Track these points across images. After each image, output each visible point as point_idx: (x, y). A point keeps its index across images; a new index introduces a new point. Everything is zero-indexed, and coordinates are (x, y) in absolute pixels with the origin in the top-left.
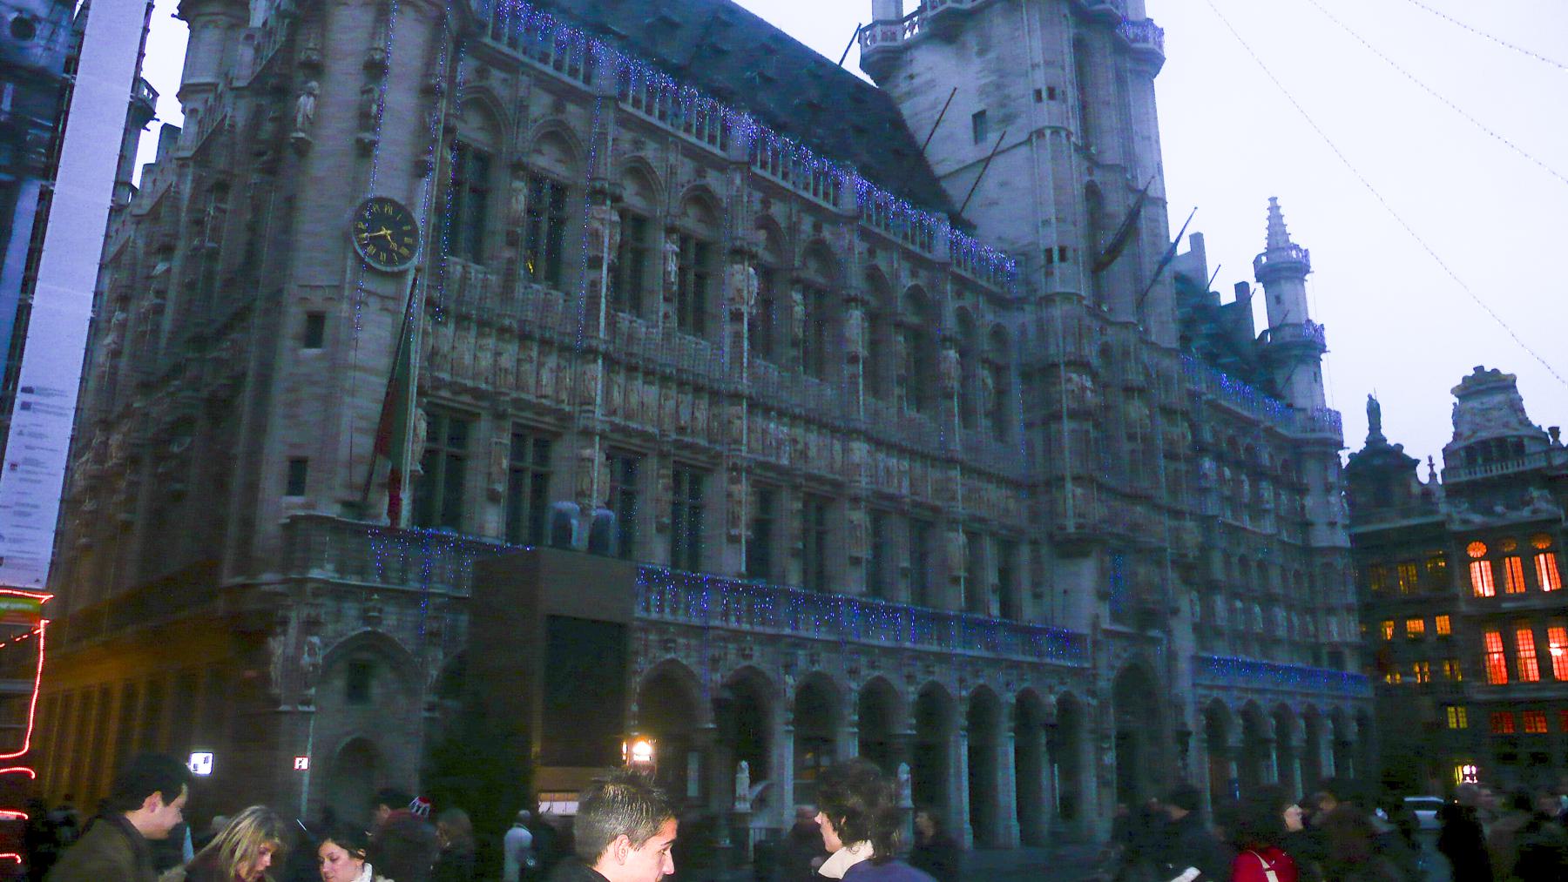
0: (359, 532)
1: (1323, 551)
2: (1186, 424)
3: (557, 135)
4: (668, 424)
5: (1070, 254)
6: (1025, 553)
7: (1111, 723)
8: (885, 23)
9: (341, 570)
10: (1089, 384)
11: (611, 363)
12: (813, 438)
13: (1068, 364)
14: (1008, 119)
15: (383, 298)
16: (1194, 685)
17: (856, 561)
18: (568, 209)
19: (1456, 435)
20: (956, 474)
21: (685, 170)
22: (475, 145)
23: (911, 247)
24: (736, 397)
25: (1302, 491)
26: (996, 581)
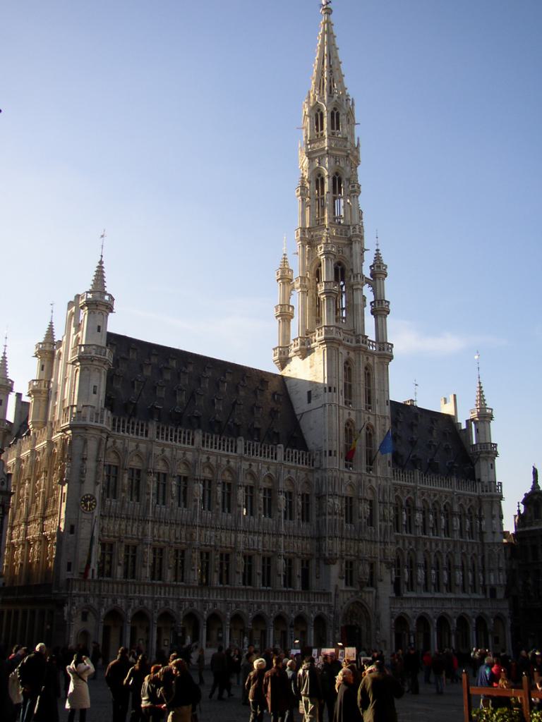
1: (489, 544)
2: (391, 508)
4: (172, 536)
6: (313, 563)
7: (341, 624)
8: (279, 347)
9: (80, 590)
10: (337, 502)
11: (154, 522)
12: (223, 535)
13: (329, 495)
14: (317, 396)
15: (88, 520)
16: (390, 608)
18: (141, 476)
20: (282, 539)
22: (113, 464)
23: (266, 460)
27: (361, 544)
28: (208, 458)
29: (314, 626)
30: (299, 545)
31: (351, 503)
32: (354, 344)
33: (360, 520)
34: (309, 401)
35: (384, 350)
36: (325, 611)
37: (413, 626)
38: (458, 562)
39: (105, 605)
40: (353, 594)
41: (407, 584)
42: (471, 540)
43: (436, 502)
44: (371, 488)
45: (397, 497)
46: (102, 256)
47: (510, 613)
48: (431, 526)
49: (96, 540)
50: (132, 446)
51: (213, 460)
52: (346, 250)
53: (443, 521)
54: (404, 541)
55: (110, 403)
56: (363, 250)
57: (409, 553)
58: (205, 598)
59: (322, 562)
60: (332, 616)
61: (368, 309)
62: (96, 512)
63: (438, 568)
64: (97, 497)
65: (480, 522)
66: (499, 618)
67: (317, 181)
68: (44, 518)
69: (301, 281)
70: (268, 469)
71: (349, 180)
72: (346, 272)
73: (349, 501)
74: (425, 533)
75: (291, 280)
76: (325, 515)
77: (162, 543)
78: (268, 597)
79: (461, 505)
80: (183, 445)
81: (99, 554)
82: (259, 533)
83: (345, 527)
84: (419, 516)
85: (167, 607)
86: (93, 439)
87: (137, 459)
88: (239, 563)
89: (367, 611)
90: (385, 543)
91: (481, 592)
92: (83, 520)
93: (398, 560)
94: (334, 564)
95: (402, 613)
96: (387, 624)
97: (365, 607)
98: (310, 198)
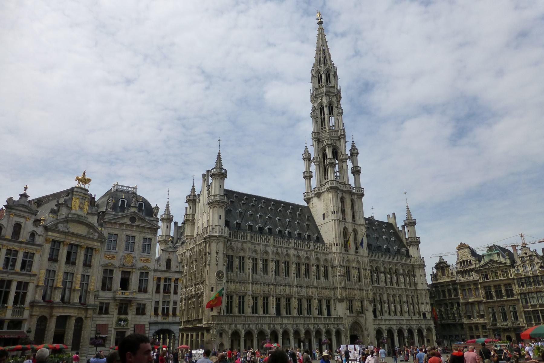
0: (220, 316)
2: (369, 272)
3: (243, 249)
5: (338, 245)
6: (332, 302)
8: (308, 192)
10: (342, 269)
11: (252, 284)
12: (287, 288)
14: (328, 216)
15: (220, 284)
17: (295, 308)
19: (458, 259)
21: (263, 248)
23: (305, 249)
24: (273, 285)
25: (414, 276)
26: (326, 308)
27: (356, 291)
28: (277, 250)
29: (335, 336)
30: (324, 293)
31: (349, 269)
32: (345, 189)
33: (354, 279)
34: (324, 218)
35: (359, 191)
36: (341, 327)
37: (385, 334)
38: (404, 299)
39: (231, 328)
40: (354, 318)
41: (380, 312)
42: (410, 288)
43: (391, 268)
44: (358, 262)
45: (371, 266)
46: (219, 150)
47: (435, 327)
48: (389, 281)
49: (224, 294)
50: (239, 245)
51: (280, 250)
52: (338, 143)
53: (395, 277)
54: (376, 289)
55: (227, 224)
56: (346, 142)
57: (379, 296)
58: (280, 323)
59: (336, 301)
60: (344, 330)
61: (350, 171)
62: (224, 279)
63: (395, 303)
64: (224, 272)
65: (414, 278)
66: (429, 330)
67: (321, 109)
68: (195, 285)
69: (316, 159)
70: (307, 254)
71: (337, 107)
72: (338, 154)
73: (348, 269)
74: (386, 284)
75: (310, 159)
76: (337, 276)
77: (257, 294)
78: (312, 321)
79: (403, 270)
80: (264, 243)
81: (226, 302)
82: (304, 287)
83: (347, 282)
84: (382, 276)
85: (262, 328)
86: (221, 242)
87: (242, 252)
88: (294, 303)
89: (361, 327)
90: (368, 290)
91: (418, 316)
92: (218, 284)
93: (374, 299)
94: (343, 302)
95: (380, 327)
96: (372, 333)
97: (360, 325)
98: (317, 117)
